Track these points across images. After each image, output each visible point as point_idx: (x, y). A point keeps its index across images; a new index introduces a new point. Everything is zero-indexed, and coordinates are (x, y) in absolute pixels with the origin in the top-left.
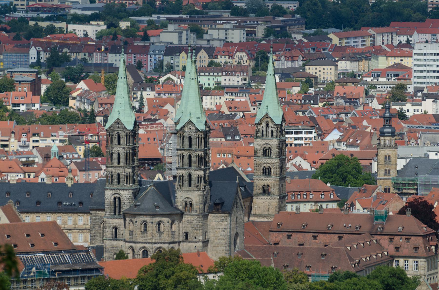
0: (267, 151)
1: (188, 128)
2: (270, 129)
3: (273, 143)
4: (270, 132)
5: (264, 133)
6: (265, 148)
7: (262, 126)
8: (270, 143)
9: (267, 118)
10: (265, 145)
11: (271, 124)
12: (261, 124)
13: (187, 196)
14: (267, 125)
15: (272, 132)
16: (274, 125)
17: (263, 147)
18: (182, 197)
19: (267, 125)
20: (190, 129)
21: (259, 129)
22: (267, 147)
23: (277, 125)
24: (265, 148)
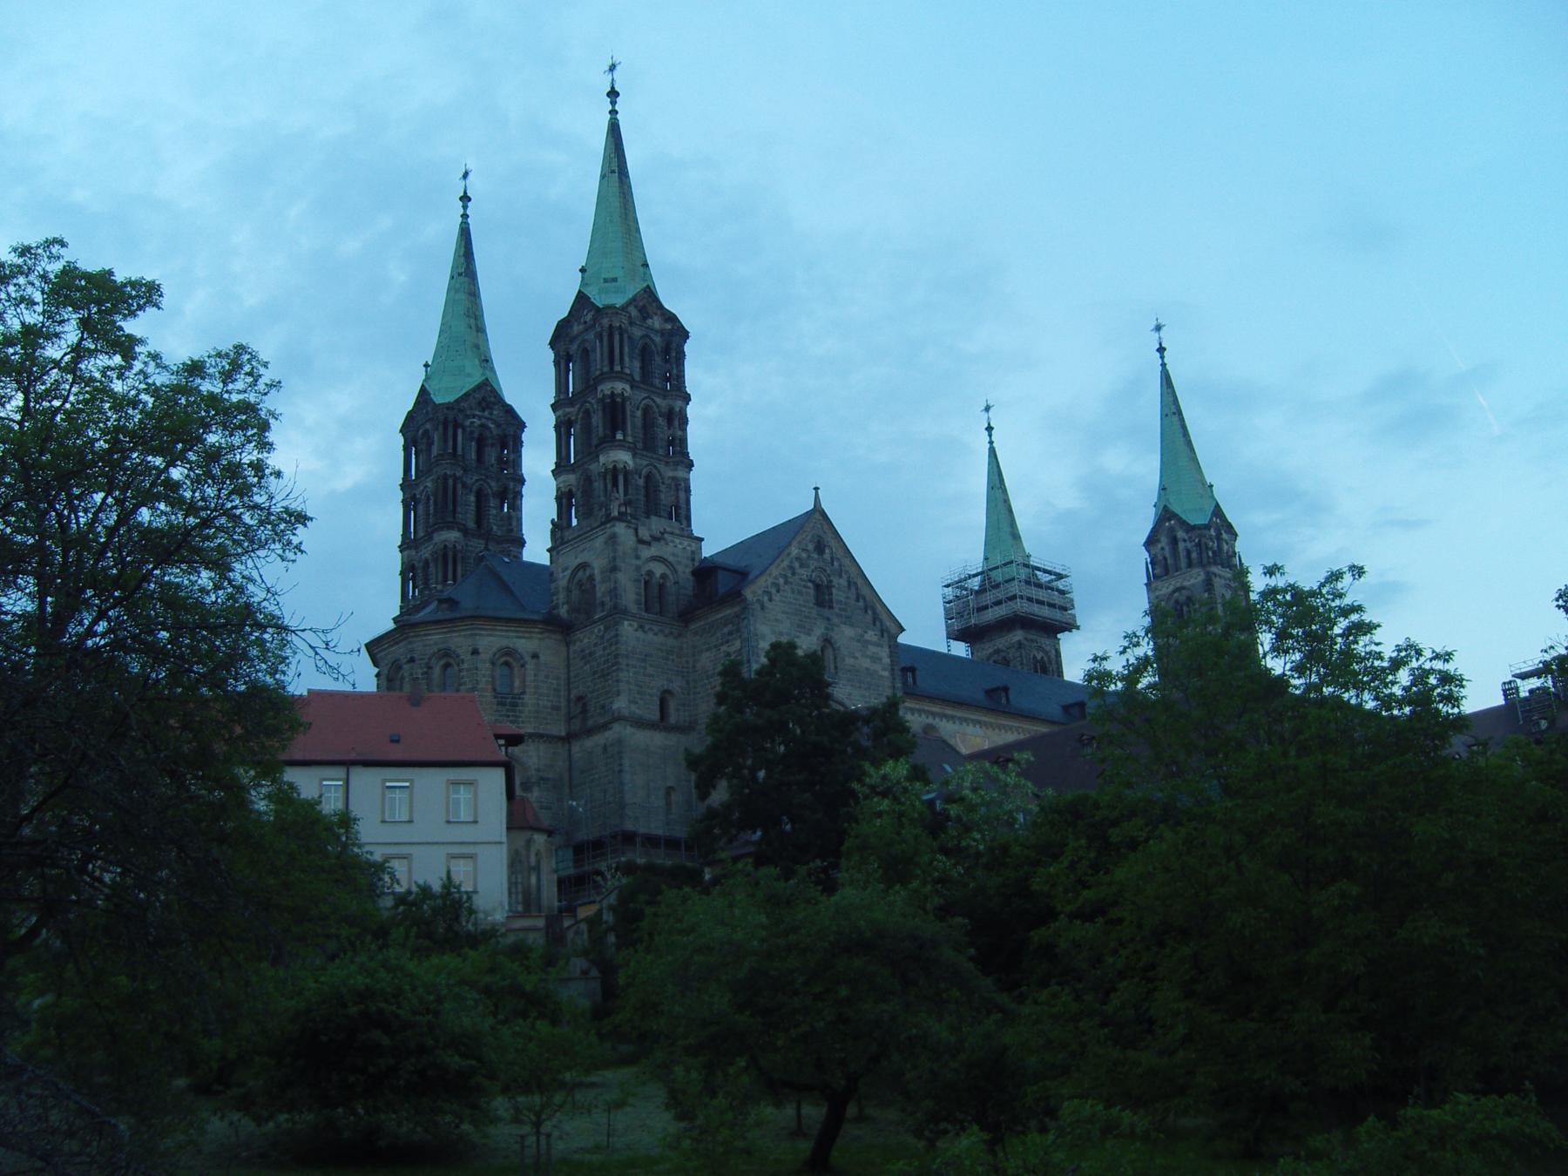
0: (1185, 609)
1: (579, 324)
2: (1181, 546)
3: (1193, 581)
4: (1182, 554)
5: (1170, 561)
6: (1177, 602)
7: (1159, 546)
8: (1186, 584)
9: (1169, 520)
10: (1176, 594)
11: (1181, 534)
12: (1158, 541)
13: (579, 561)
14: (1174, 541)
15: (1189, 553)
16: (1187, 532)
17: (1172, 602)
18: (564, 570)
19: (1174, 541)
20: (585, 322)
21: (1155, 555)
22: (1182, 599)
23: (1194, 528)
24: (1177, 602)
